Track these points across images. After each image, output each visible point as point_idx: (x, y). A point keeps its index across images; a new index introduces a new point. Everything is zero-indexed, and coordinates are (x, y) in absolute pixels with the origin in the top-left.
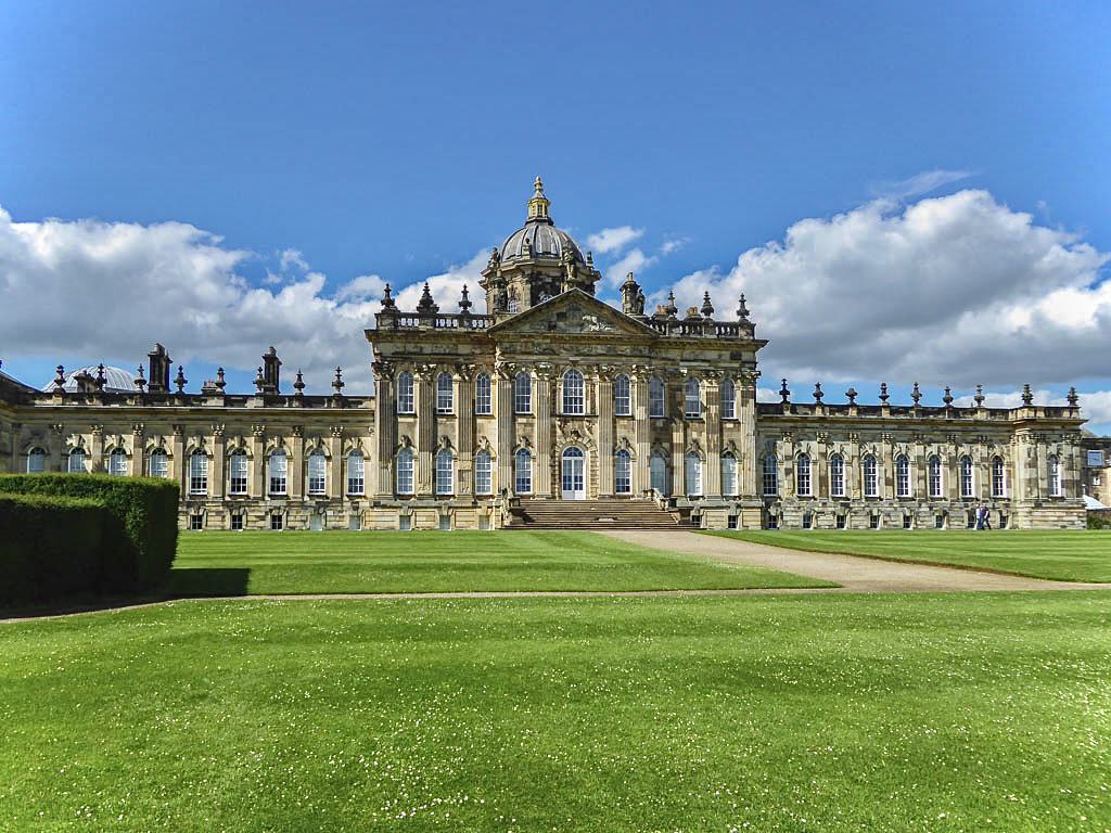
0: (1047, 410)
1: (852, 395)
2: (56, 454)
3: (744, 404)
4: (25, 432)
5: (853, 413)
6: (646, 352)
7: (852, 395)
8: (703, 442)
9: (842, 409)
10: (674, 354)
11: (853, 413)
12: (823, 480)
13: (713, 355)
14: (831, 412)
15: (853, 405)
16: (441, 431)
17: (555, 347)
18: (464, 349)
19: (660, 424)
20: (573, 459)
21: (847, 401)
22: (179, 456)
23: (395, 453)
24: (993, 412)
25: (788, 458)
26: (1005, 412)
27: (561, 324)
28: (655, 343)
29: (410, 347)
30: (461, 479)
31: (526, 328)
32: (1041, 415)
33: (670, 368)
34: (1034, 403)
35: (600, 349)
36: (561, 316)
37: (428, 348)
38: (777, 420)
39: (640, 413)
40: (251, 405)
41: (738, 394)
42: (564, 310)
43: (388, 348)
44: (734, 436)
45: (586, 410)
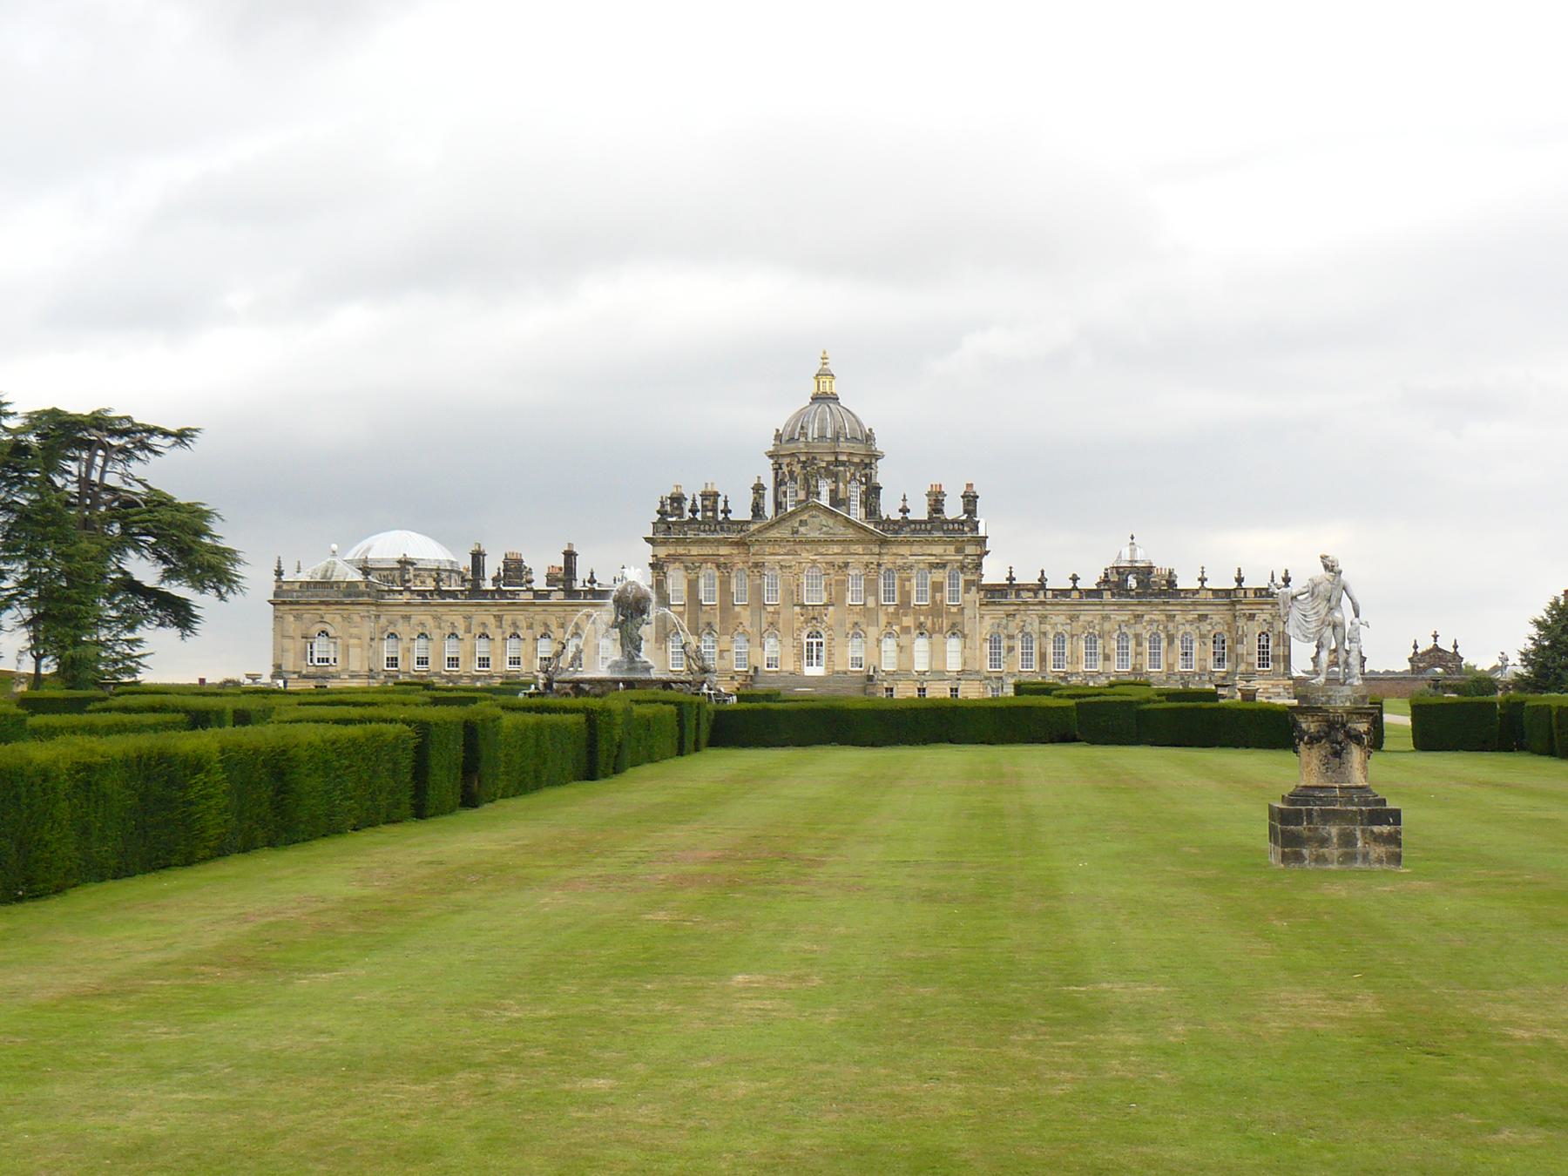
0: (1258, 592)
1: (1075, 579)
2: (406, 639)
3: (967, 591)
4: (383, 621)
5: (1075, 594)
6: (876, 550)
7: (1075, 579)
8: (929, 624)
9: (1065, 593)
10: (904, 550)
11: (1075, 594)
12: (1043, 658)
13: (938, 550)
14: (1055, 596)
15: (1075, 588)
16: (703, 618)
17: (797, 547)
18: (724, 550)
19: (891, 610)
20: (815, 641)
21: (1070, 585)
22: (499, 638)
23: (667, 636)
24: (1215, 591)
25: (1010, 637)
26: (1228, 592)
27: (802, 529)
28: (883, 542)
29: (681, 550)
30: (721, 657)
31: (774, 534)
32: (1251, 594)
33: (900, 562)
34: (1244, 585)
35: (836, 549)
36: (802, 523)
37: (695, 550)
38: (1000, 604)
39: (871, 603)
40: (553, 600)
41: (962, 584)
42: (805, 517)
43: (662, 552)
44: (958, 619)
45: (825, 600)
